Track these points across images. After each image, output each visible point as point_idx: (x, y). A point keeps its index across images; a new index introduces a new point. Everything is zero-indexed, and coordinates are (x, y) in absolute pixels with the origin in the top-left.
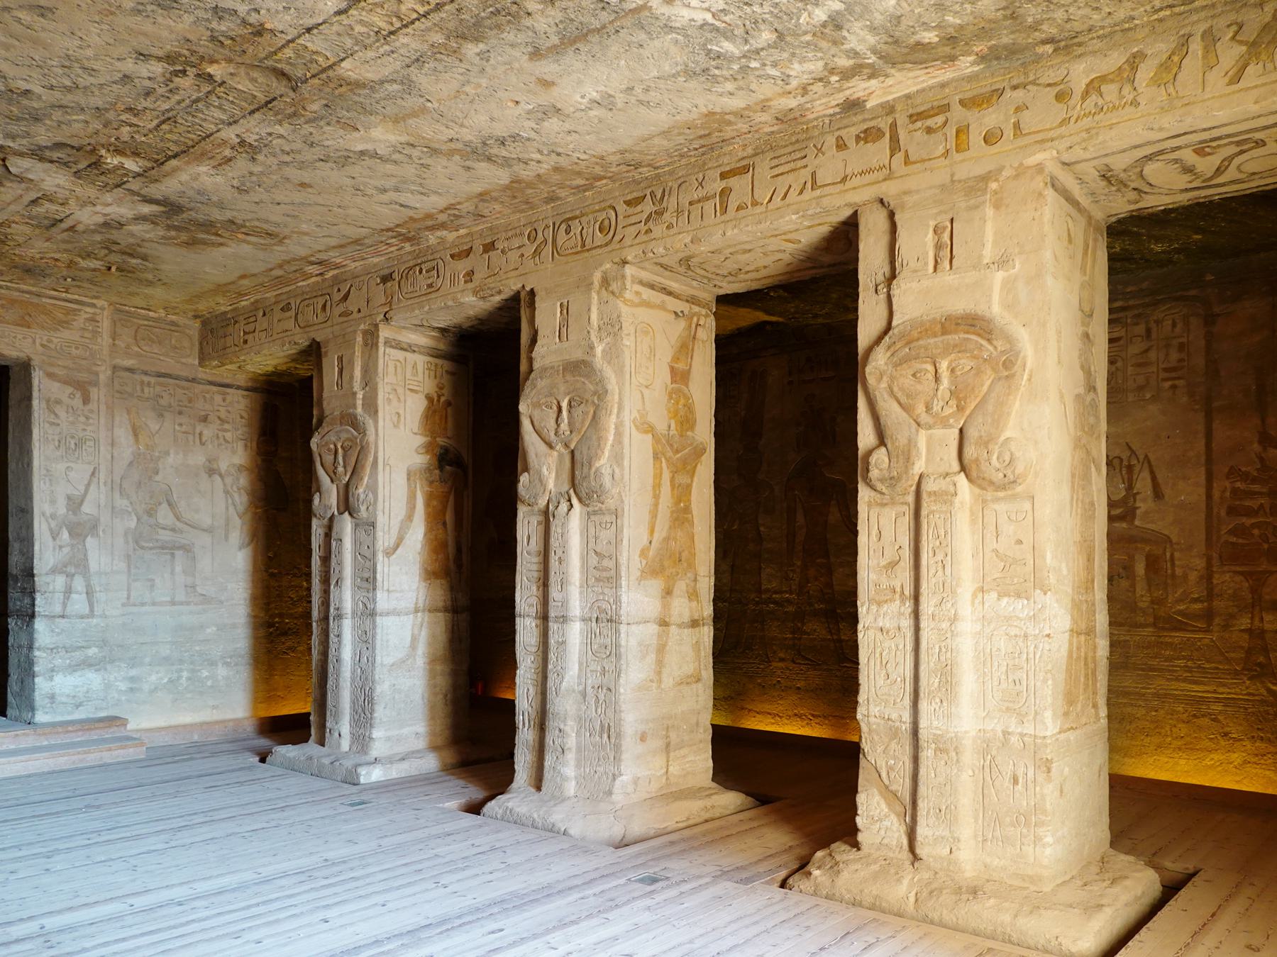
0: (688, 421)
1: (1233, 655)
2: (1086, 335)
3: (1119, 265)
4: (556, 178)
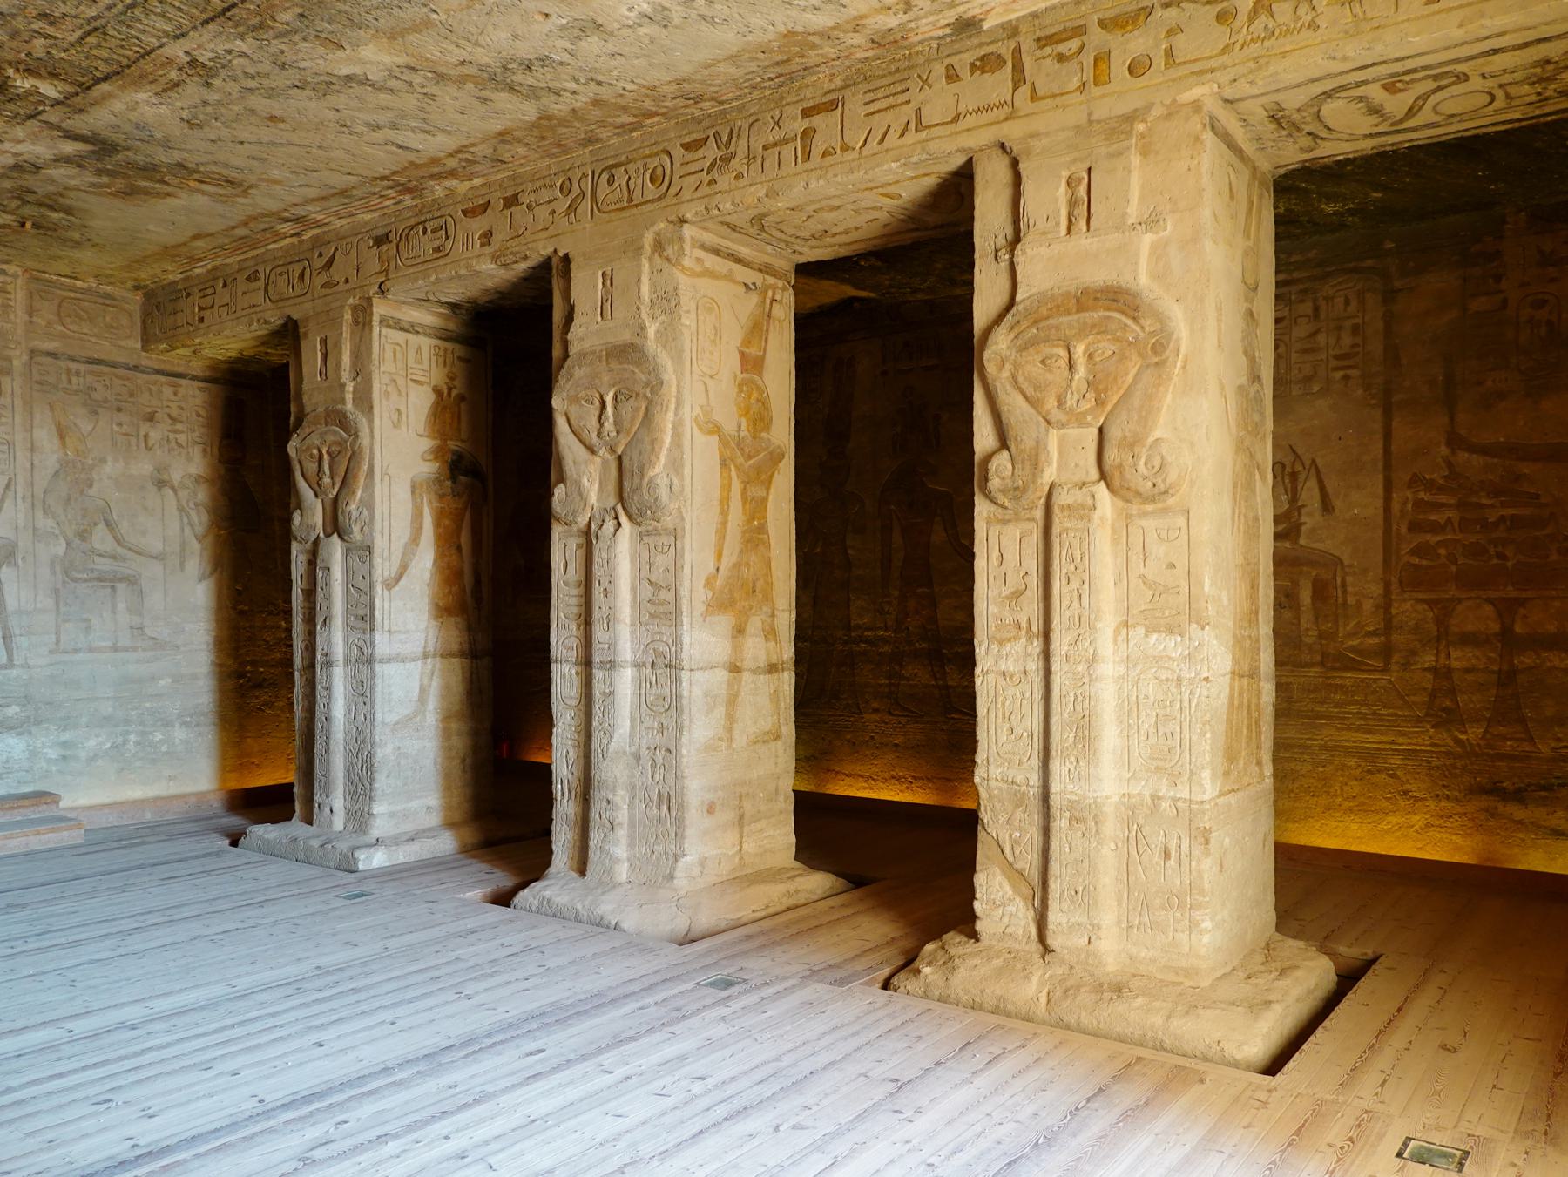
0: (762, 419)
1: (1413, 698)
2: (1250, 314)
3: (1287, 228)
4: (596, 113)
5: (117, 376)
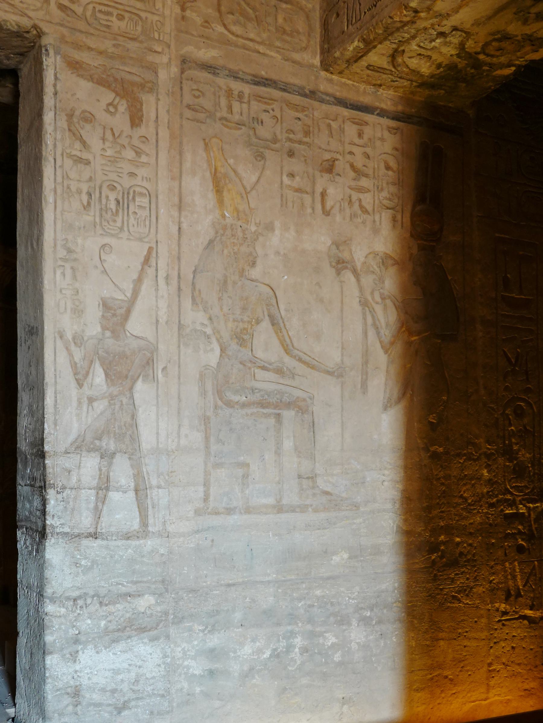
5: (289, 104)
